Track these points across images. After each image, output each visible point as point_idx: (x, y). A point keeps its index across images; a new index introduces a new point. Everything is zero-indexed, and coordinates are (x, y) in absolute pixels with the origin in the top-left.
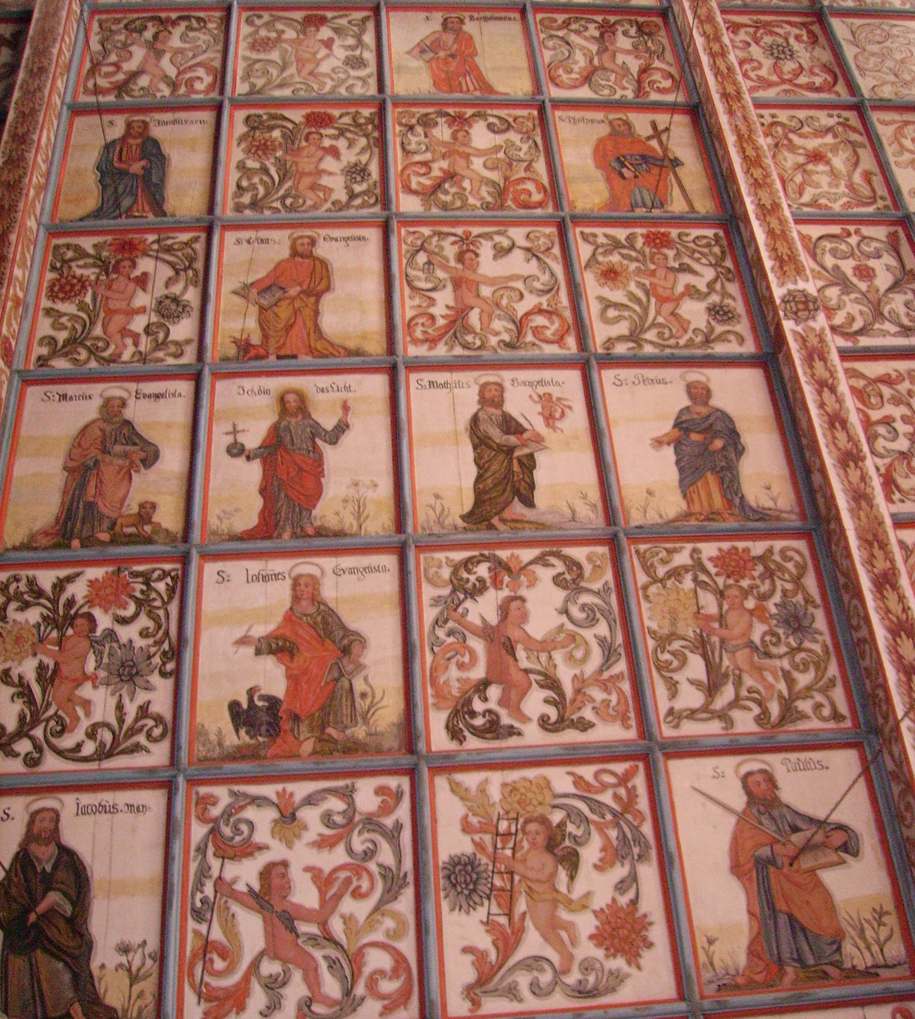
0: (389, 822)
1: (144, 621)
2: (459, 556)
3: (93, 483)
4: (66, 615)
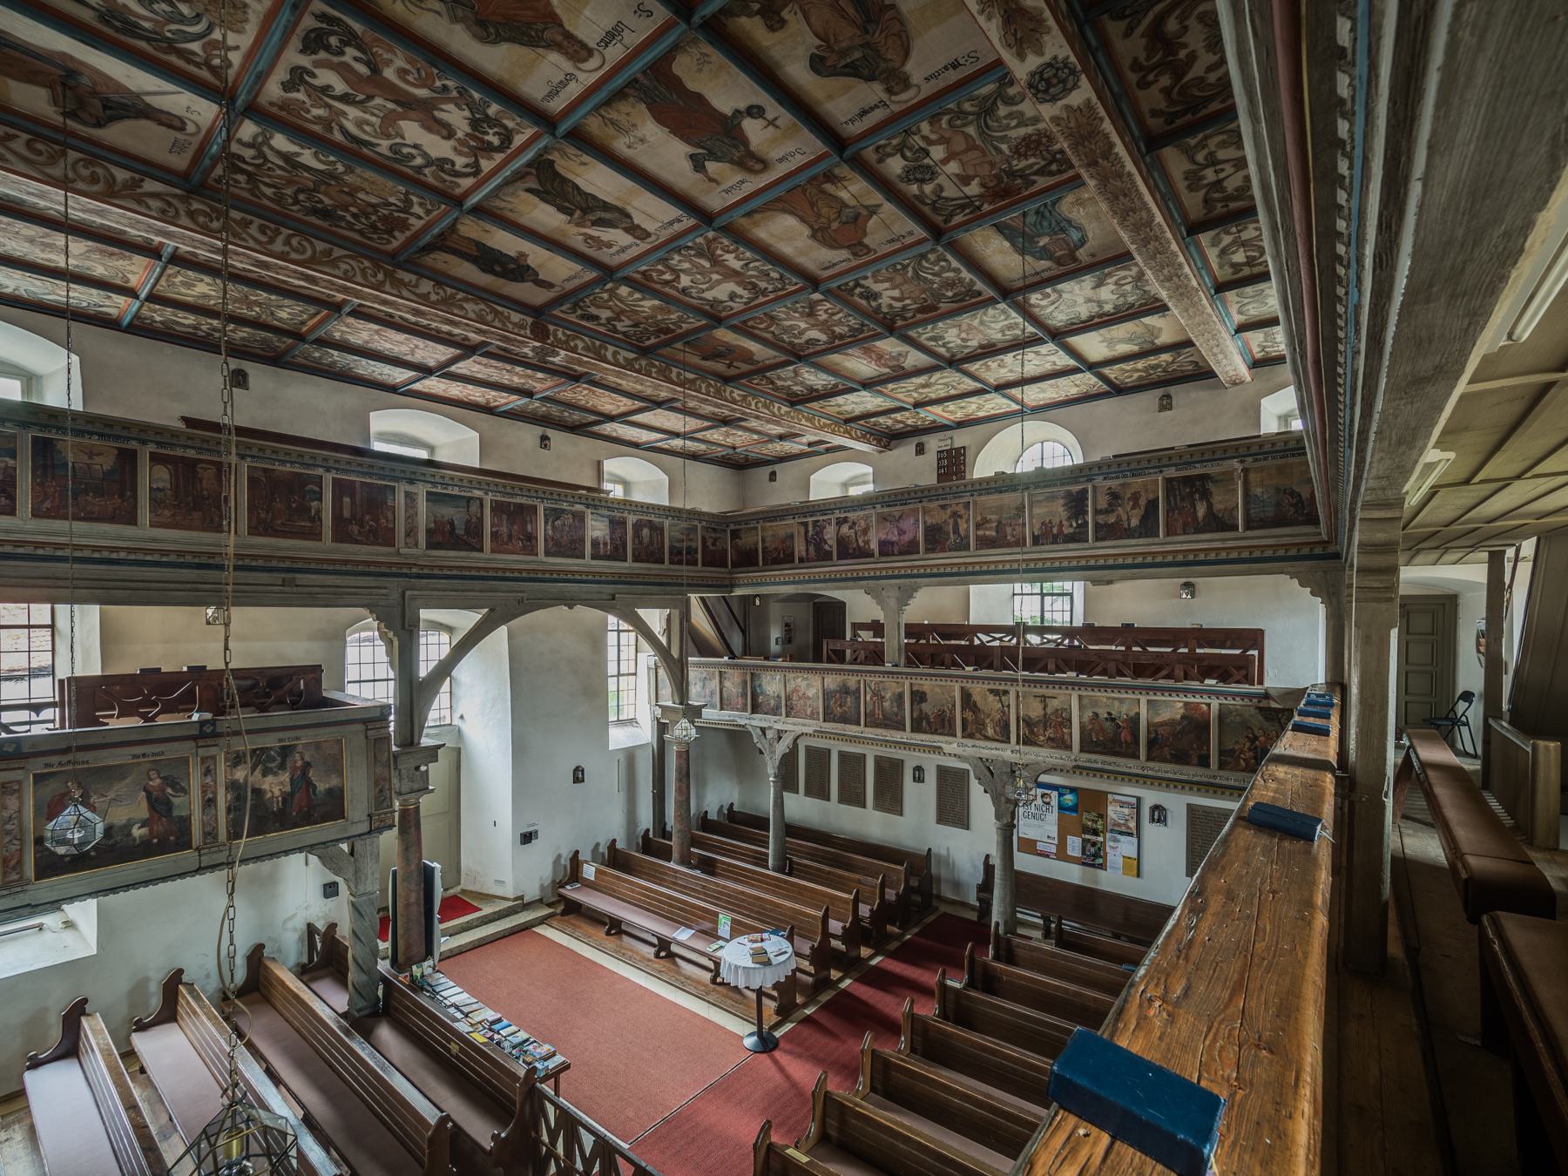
3: (851, 11)
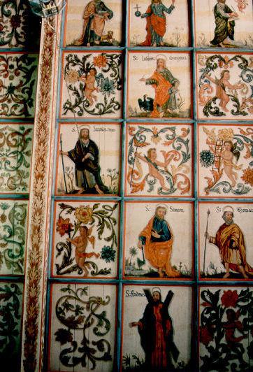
0: (185, 139)
1: (111, 72)
2: (209, 55)
3: (92, 24)
4: (87, 68)
